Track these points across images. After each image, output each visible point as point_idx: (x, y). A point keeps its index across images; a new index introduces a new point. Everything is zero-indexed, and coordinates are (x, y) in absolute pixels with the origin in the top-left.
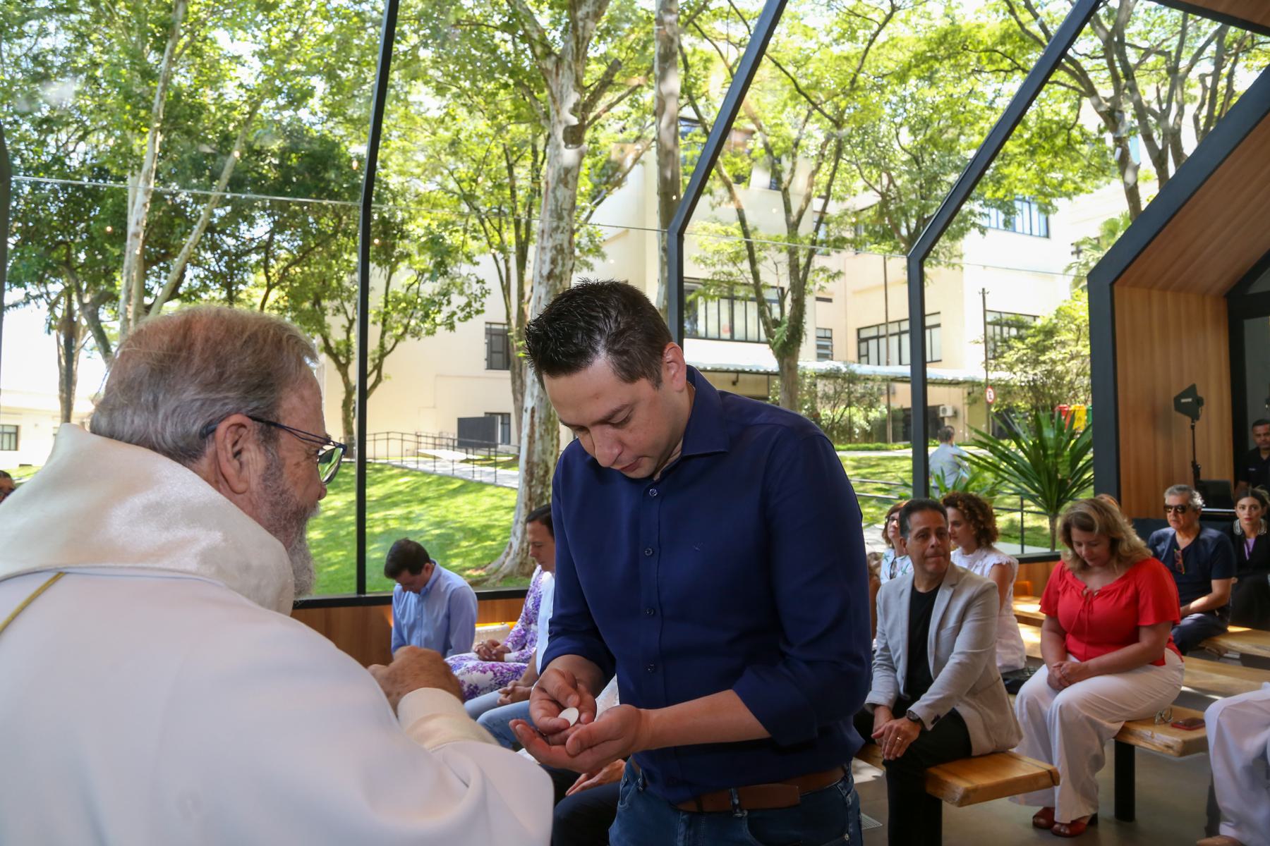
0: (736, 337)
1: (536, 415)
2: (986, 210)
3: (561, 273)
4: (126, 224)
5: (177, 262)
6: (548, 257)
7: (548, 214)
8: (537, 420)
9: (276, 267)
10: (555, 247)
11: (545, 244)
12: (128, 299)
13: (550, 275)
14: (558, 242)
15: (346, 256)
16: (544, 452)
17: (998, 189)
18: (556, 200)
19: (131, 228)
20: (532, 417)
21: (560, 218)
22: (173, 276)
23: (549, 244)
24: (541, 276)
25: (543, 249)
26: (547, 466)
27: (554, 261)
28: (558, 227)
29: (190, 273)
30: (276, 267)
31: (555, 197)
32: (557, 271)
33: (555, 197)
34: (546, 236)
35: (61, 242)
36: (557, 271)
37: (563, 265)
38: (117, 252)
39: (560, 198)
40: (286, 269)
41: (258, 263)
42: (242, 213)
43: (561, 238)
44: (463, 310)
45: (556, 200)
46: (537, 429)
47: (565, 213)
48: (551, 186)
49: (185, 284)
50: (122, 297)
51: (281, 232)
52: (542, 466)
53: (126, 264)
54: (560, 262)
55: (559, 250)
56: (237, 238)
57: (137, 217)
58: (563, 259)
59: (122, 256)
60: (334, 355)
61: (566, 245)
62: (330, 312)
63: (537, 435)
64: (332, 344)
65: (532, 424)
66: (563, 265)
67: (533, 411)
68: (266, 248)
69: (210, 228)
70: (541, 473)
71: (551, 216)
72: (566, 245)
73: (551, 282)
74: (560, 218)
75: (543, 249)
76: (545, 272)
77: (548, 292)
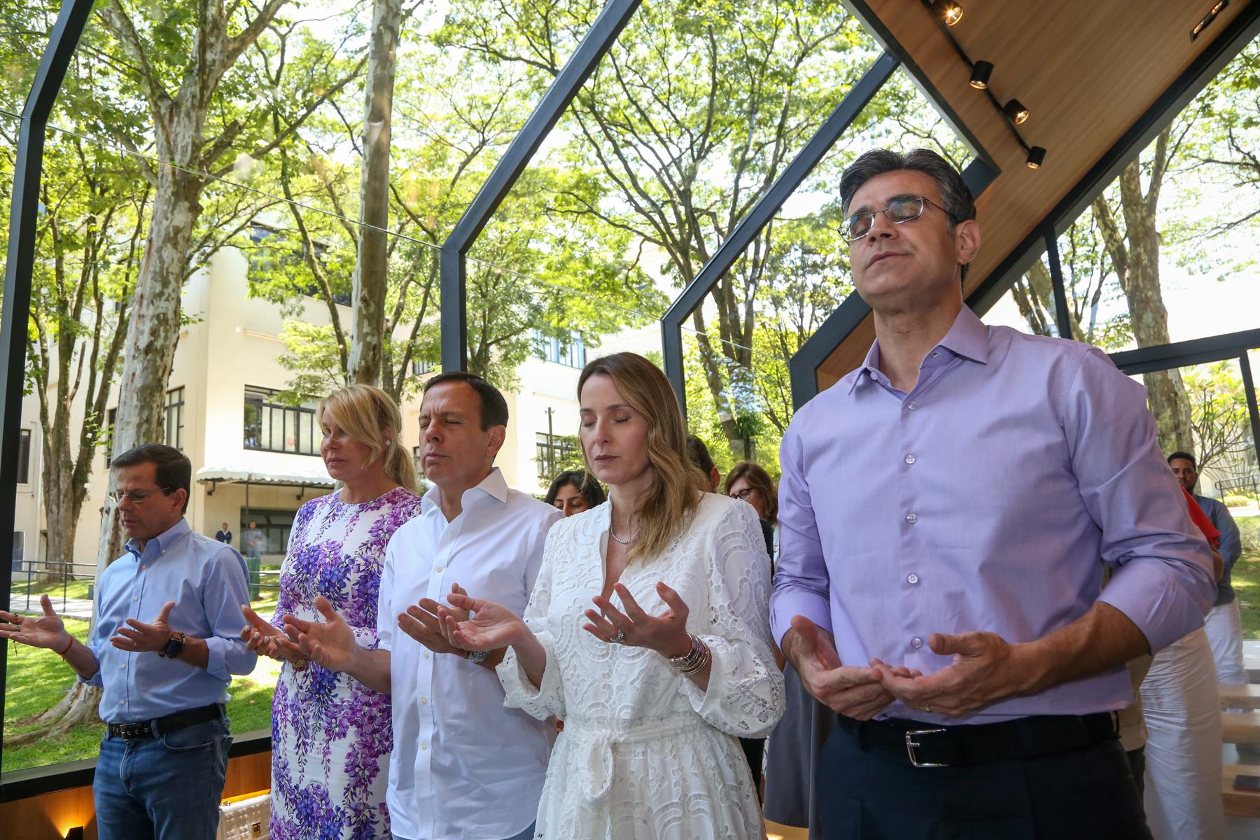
0: (302, 449)
2: (547, 339)
3: (163, 347)
6: (147, 326)
7: (150, 276)
10: (158, 317)
11: (144, 311)
13: (149, 349)
14: (160, 310)
17: (562, 319)
18: (162, 262)
21: (165, 284)
23: (149, 312)
24: (137, 349)
25: (141, 317)
27: (154, 333)
28: (161, 294)
31: (160, 258)
32: (158, 344)
33: (160, 258)
34: (145, 302)
39: (168, 261)
43: (164, 306)
45: (162, 262)
47: (171, 278)
48: (156, 245)
54: (162, 335)
55: (162, 320)
58: (166, 331)
61: (170, 315)
66: (166, 338)
71: (154, 278)
72: (170, 315)
74: (165, 284)
75: (141, 317)
76: (143, 343)
77: (145, 369)
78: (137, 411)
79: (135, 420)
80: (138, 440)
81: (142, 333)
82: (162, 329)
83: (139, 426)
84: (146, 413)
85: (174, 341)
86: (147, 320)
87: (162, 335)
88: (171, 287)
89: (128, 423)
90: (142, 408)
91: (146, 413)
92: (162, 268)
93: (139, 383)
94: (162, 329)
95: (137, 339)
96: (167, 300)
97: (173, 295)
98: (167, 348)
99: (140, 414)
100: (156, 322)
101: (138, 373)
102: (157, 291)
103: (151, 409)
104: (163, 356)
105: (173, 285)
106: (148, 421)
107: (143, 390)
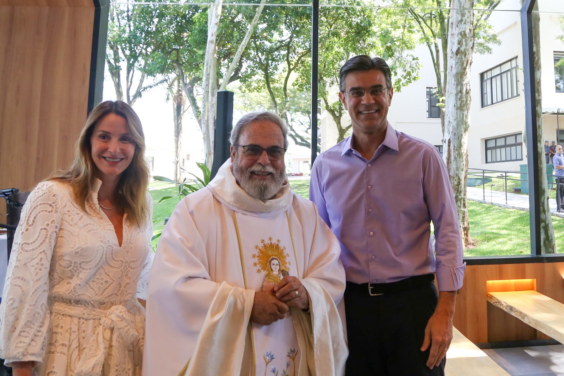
1: (452, 145)
3: (465, 50)
4: (207, 36)
5: (236, 58)
8: (452, 148)
9: (294, 58)
11: (454, 32)
12: (208, 79)
13: (458, 52)
14: (462, 30)
15: (336, 49)
16: (457, 169)
19: (210, 38)
20: (449, 146)
21: (463, 15)
22: (233, 65)
24: (452, 53)
26: (459, 179)
27: (460, 43)
28: (462, 20)
29: (245, 65)
30: (294, 58)
34: (454, 26)
35: (175, 49)
36: (462, 49)
37: (466, 45)
38: (200, 52)
40: (300, 58)
41: (284, 55)
42: (273, 26)
44: (405, 78)
46: (452, 153)
49: (243, 70)
50: (204, 79)
51: (297, 37)
52: (456, 178)
53: (206, 59)
54: (464, 43)
56: (270, 41)
57: (212, 30)
58: (466, 41)
59: (204, 55)
60: (332, 112)
62: (328, 84)
63: (452, 158)
64: (330, 104)
65: (449, 151)
66: (466, 45)
67: (449, 142)
68: (288, 46)
69: (255, 37)
70: (456, 183)
73: (459, 56)
74: (463, 15)
76: (455, 50)
78: (455, 87)
79: (454, 92)
80: (456, 103)
81: (454, 44)
82: (464, 40)
83: (457, 94)
84: (459, 88)
85: (471, 45)
86: (455, 36)
87: (464, 43)
88: (466, 16)
89: (451, 93)
90: (457, 85)
91: (459, 88)
92: (460, 7)
93: (454, 71)
94: (464, 40)
95: (452, 47)
96: (465, 23)
97: (468, 20)
98: (468, 50)
99: (456, 88)
100: (460, 37)
101: (454, 66)
102: (459, 19)
103: (462, 85)
104: (465, 55)
105: (467, 14)
106: (461, 92)
107: (457, 74)
